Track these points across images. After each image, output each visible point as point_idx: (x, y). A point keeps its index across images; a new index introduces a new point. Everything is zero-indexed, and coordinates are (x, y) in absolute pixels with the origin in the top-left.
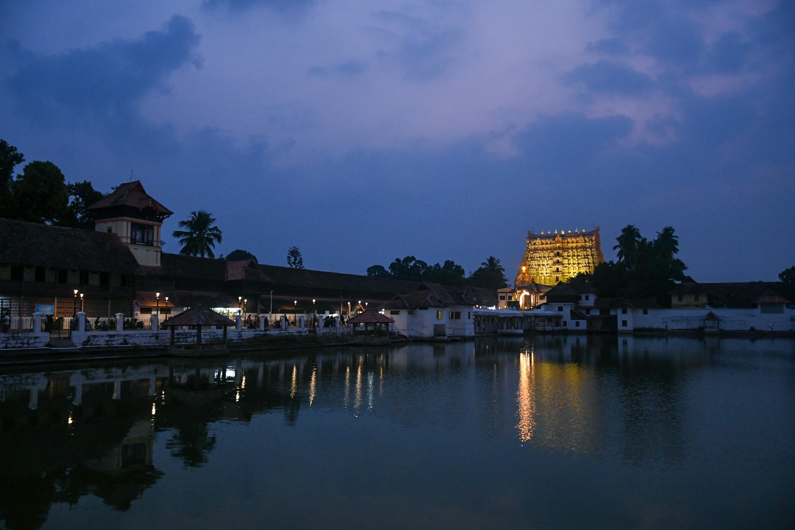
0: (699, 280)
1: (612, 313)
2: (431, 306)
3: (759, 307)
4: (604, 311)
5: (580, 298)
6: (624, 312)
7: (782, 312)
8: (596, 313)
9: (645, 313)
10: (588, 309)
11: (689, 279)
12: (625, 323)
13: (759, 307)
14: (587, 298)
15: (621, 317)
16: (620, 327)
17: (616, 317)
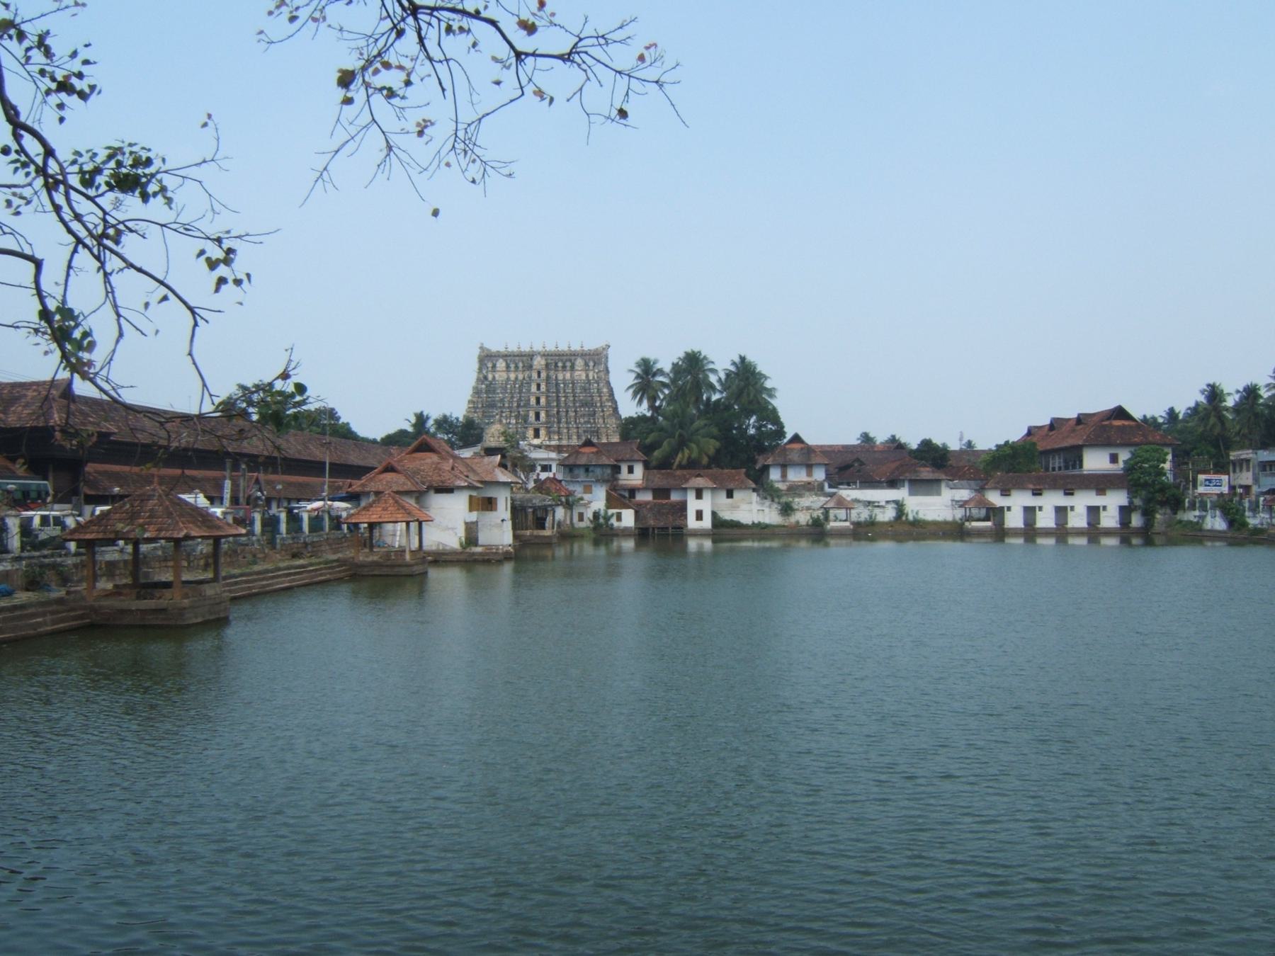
0: (811, 439)
1: (675, 497)
2: (461, 488)
3: (907, 484)
4: (662, 493)
5: (616, 469)
6: (699, 495)
7: (939, 494)
8: (645, 497)
9: (730, 495)
10: (632, 491)
11: (796, 439)
12: (699, 515)
13: (907, 484)
14: (631, 470)
15: (693, 505)
16: (692, 523)
17: (683, 507)
